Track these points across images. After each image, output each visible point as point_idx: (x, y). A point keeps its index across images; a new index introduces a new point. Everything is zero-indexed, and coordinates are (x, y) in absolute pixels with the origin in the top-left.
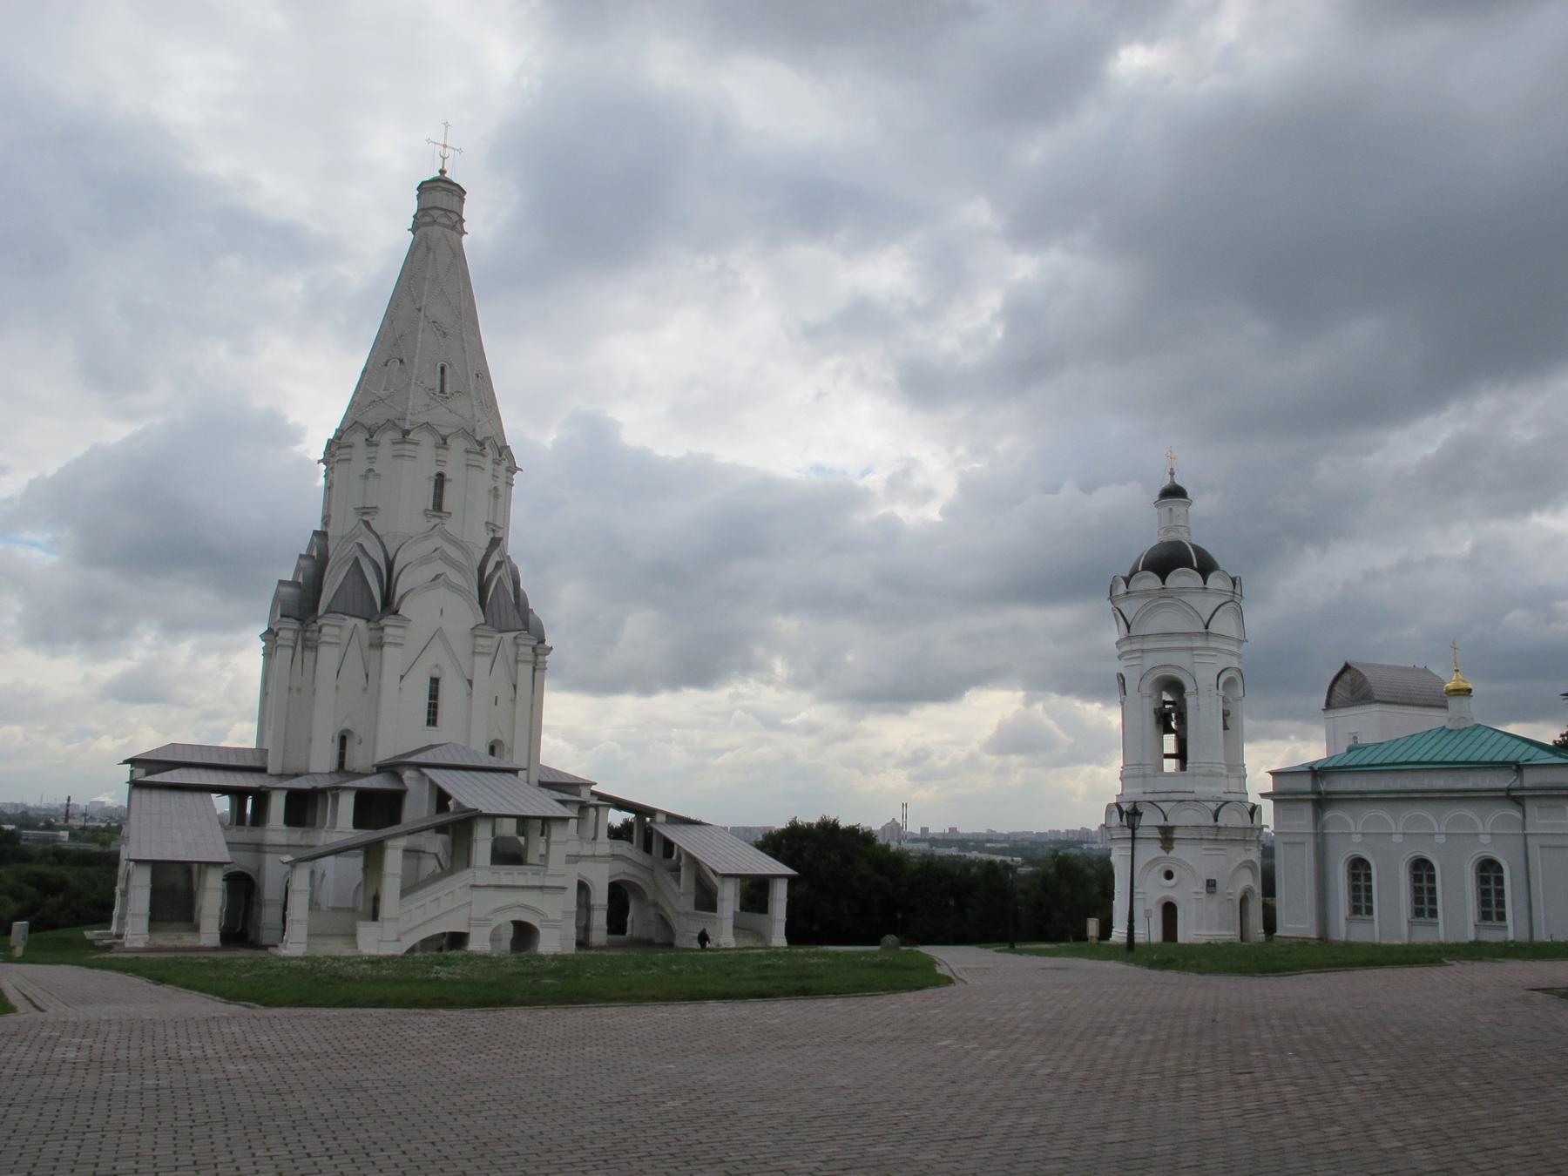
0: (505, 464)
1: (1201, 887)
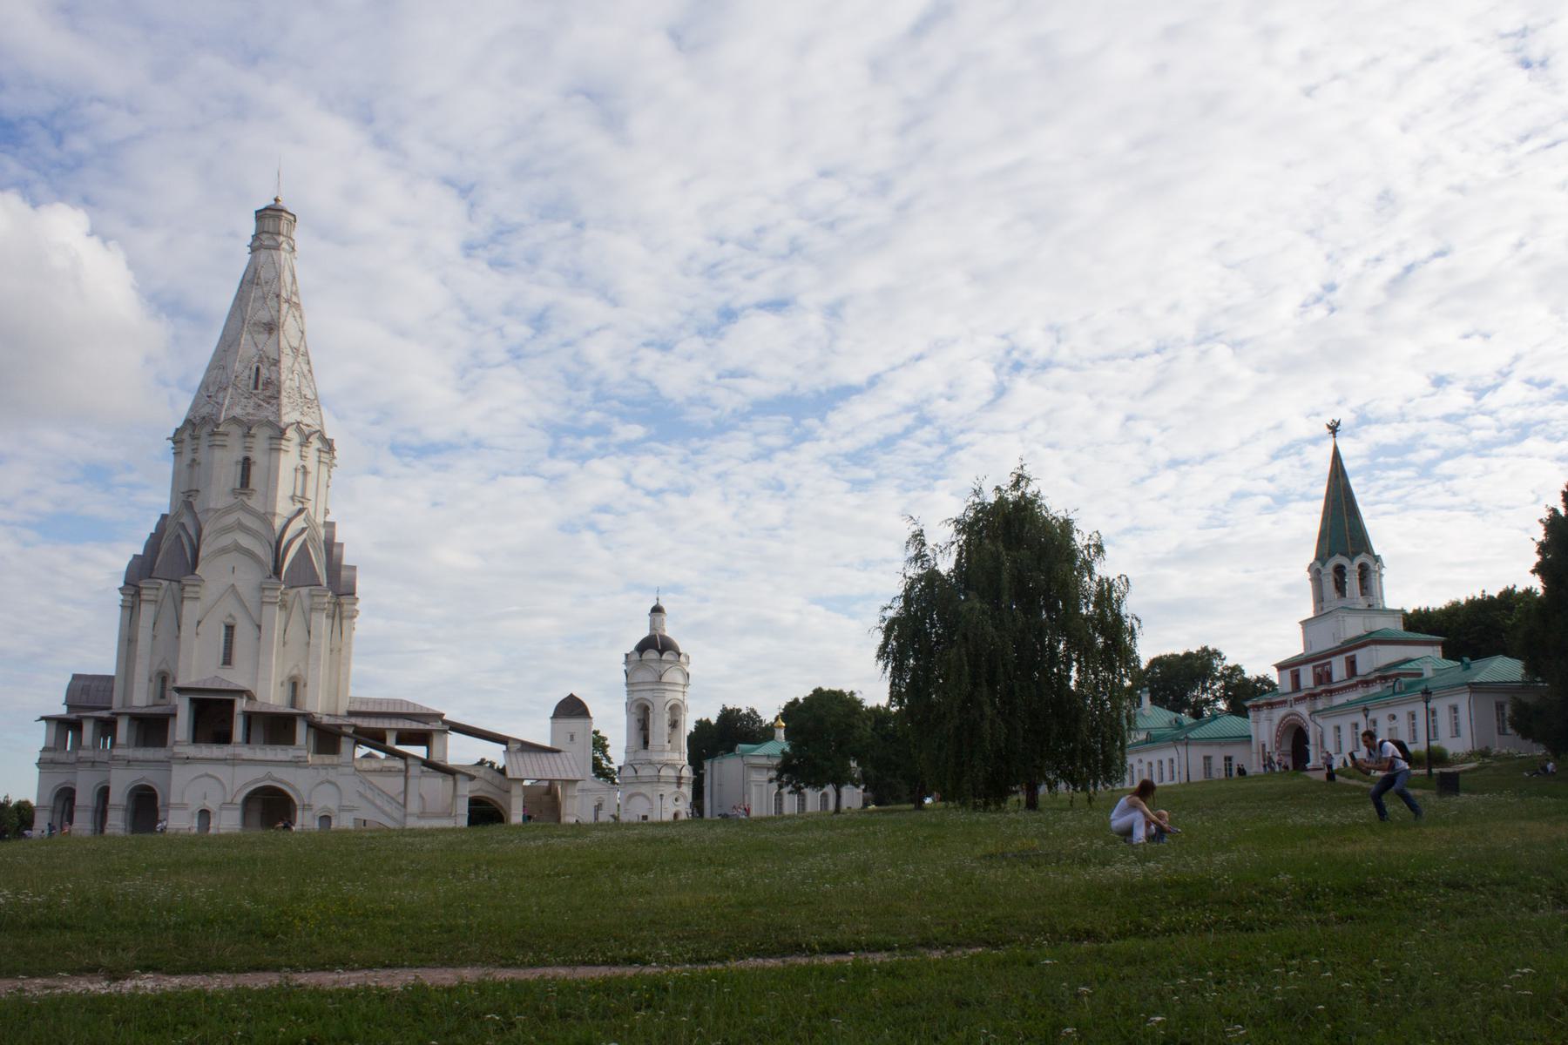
0: (315, 443)
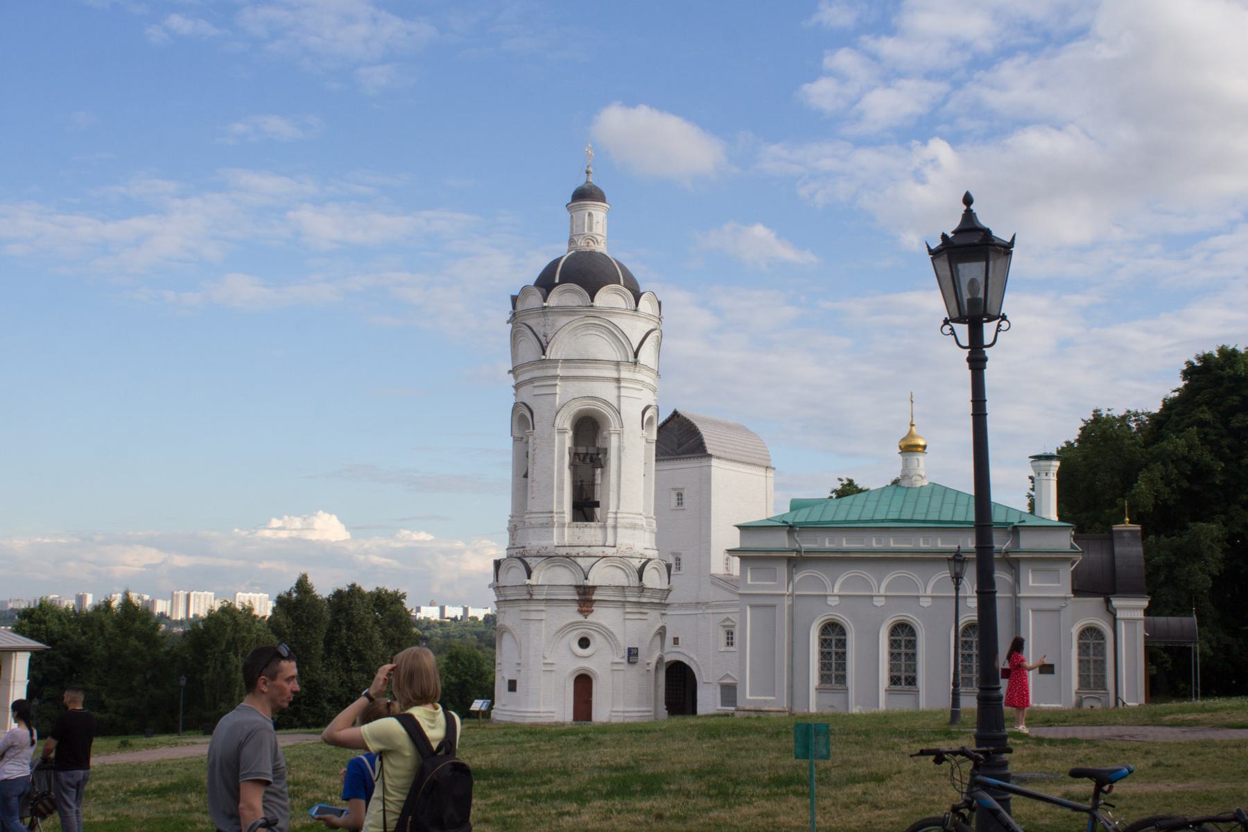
1: (621, 657)
